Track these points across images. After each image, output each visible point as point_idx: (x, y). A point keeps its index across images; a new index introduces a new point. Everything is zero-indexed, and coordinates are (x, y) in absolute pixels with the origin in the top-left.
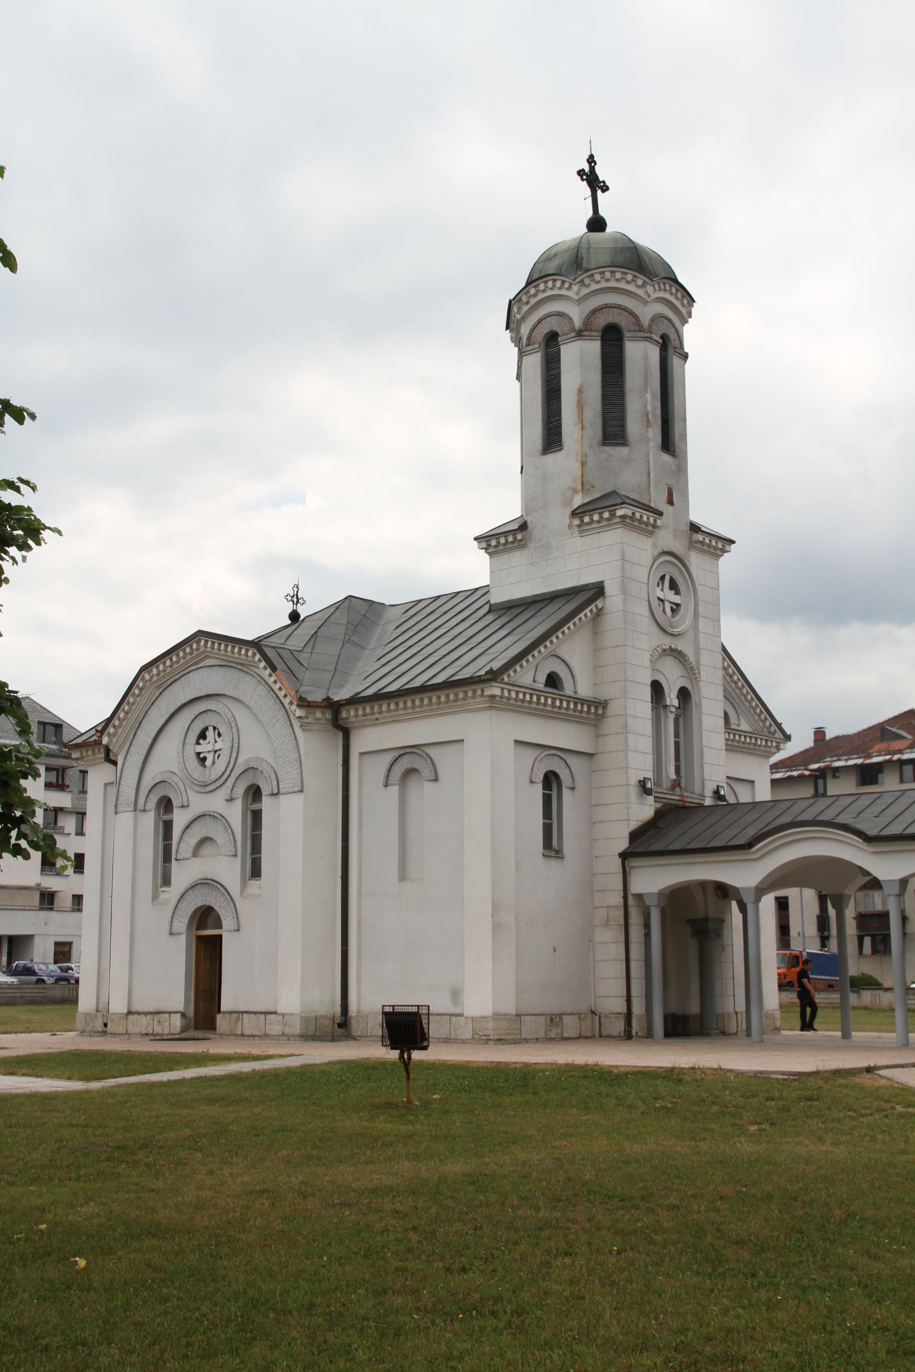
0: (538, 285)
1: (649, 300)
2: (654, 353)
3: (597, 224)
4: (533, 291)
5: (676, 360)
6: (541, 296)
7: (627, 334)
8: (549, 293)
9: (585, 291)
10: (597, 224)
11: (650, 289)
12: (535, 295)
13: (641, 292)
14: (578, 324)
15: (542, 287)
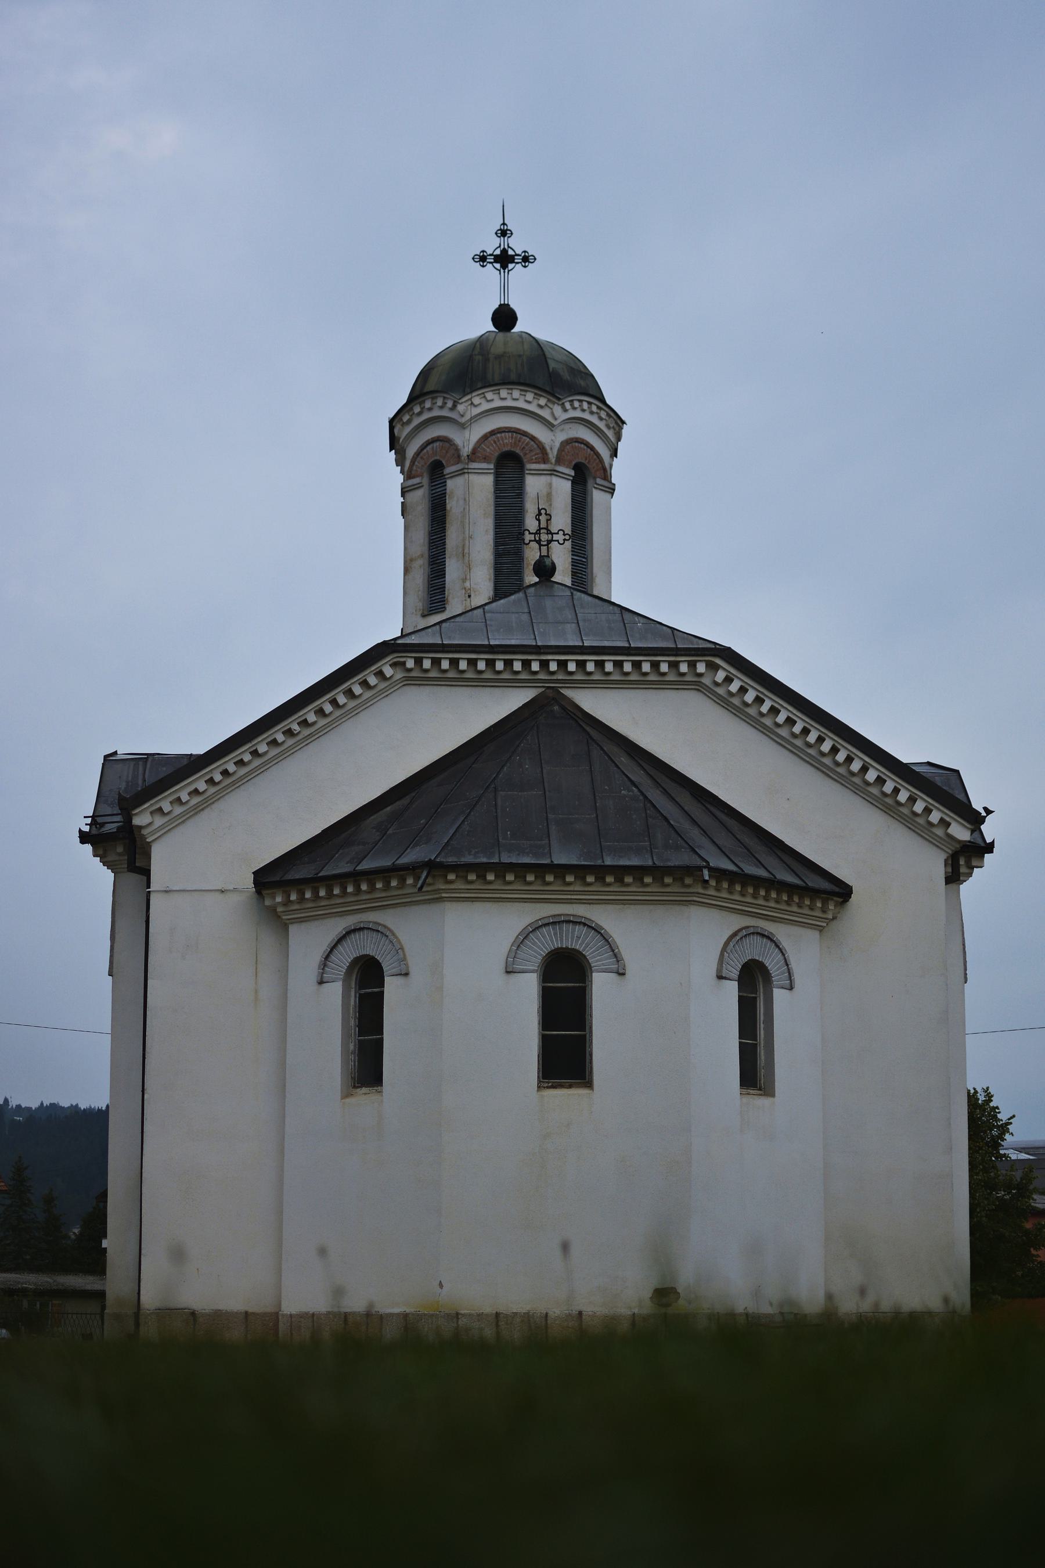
0: (424, 402)
1: (555, 423)
2: (563, 488)
3: (504, 318)
4: (417, 409)
5: (597, 496)
6: (426, 416)
7: (529, 466)
8: (436, 413)
9: (476, 411)
10: (504, 318)
11: (557, 409)
12: (420, 414)
13: (545, 413)
14: (466, 451)
15: (428, 404)
